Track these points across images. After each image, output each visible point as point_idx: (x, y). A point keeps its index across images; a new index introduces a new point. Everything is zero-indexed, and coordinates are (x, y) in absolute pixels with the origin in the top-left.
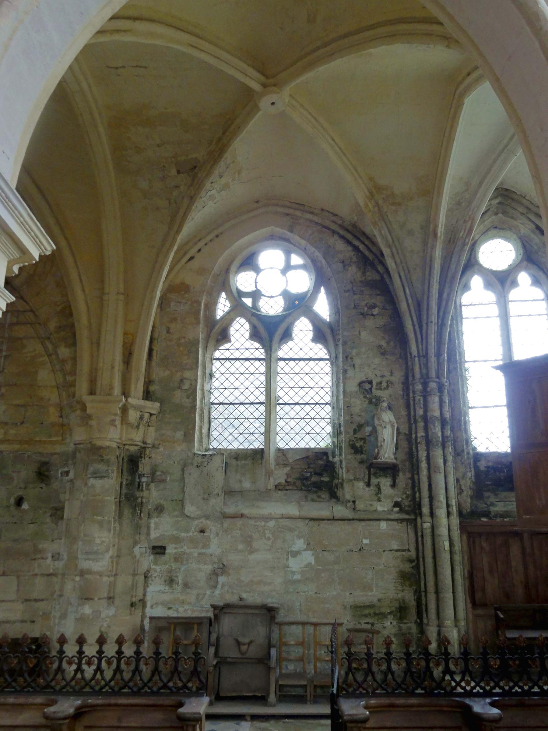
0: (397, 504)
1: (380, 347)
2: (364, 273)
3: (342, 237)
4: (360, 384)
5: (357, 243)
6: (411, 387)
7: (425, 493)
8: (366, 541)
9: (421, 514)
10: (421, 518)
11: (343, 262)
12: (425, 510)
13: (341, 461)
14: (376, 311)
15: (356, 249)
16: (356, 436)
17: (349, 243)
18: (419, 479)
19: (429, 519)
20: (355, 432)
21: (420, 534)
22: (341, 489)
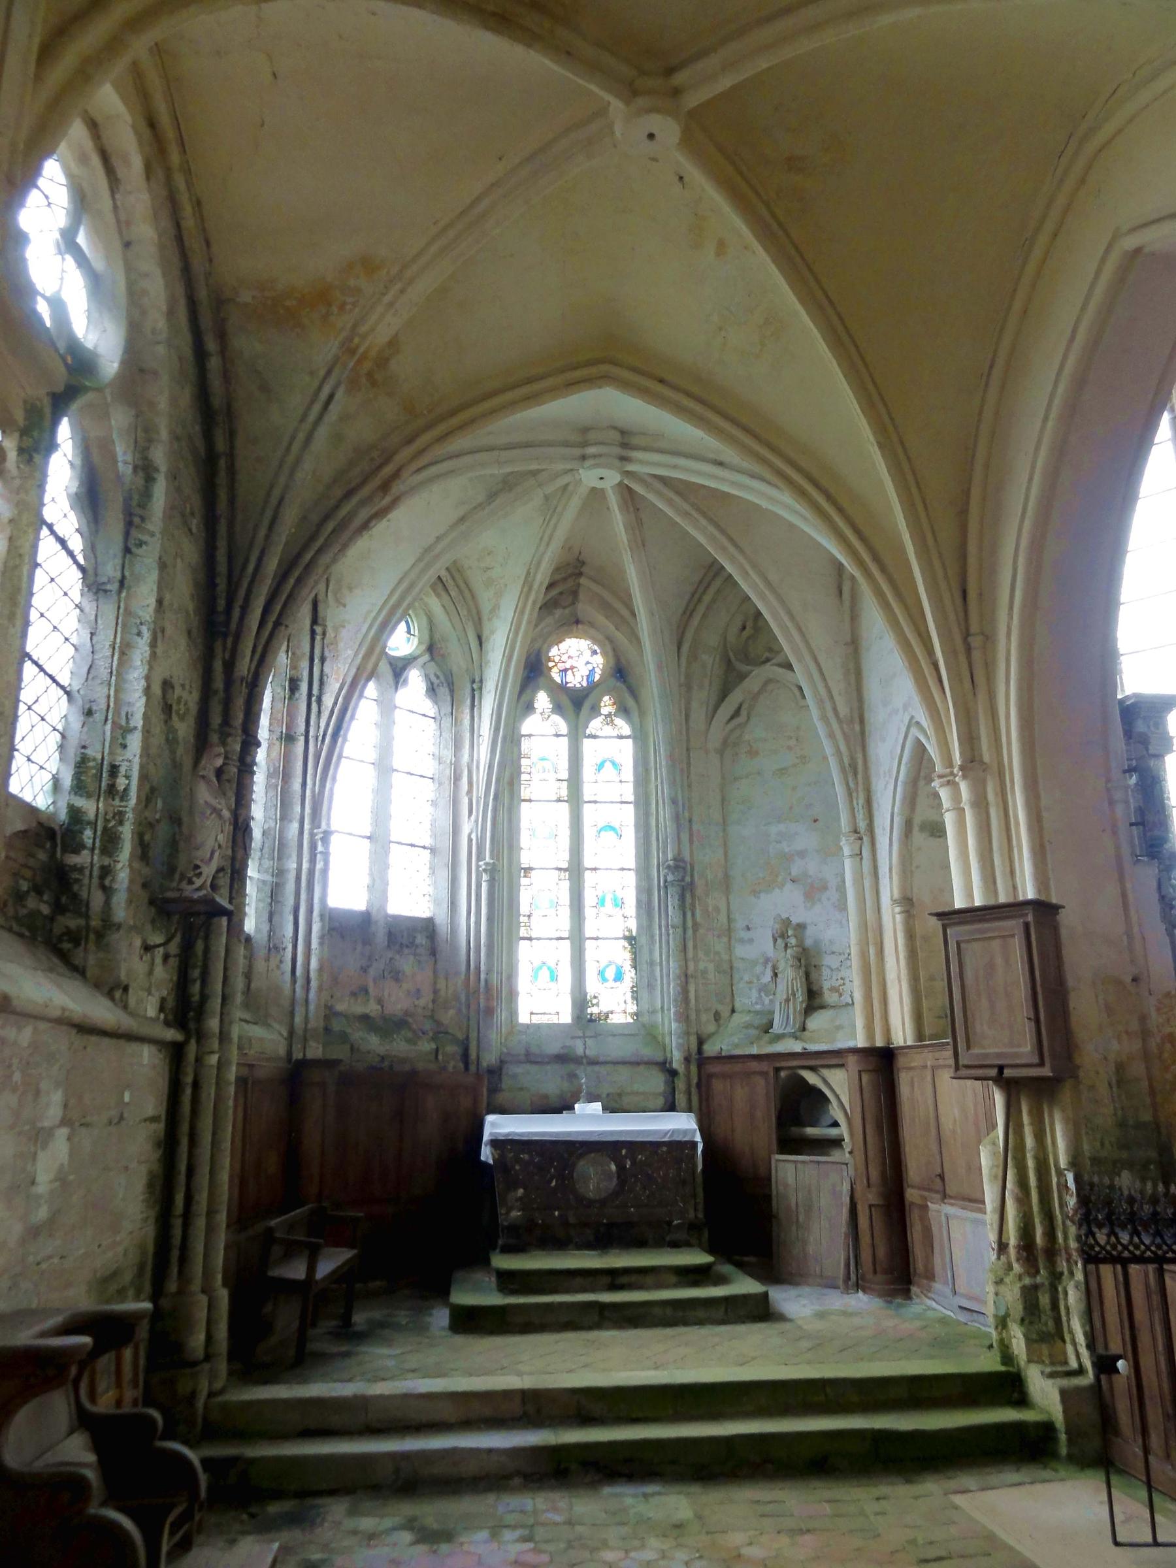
9: (201, 1036)
10: (198, 1042)
12: (213, 1024)
13: (106, 871)
16: (147, 814)
18: (207, 950)
19: (216, 1046)
22: (92, 946)
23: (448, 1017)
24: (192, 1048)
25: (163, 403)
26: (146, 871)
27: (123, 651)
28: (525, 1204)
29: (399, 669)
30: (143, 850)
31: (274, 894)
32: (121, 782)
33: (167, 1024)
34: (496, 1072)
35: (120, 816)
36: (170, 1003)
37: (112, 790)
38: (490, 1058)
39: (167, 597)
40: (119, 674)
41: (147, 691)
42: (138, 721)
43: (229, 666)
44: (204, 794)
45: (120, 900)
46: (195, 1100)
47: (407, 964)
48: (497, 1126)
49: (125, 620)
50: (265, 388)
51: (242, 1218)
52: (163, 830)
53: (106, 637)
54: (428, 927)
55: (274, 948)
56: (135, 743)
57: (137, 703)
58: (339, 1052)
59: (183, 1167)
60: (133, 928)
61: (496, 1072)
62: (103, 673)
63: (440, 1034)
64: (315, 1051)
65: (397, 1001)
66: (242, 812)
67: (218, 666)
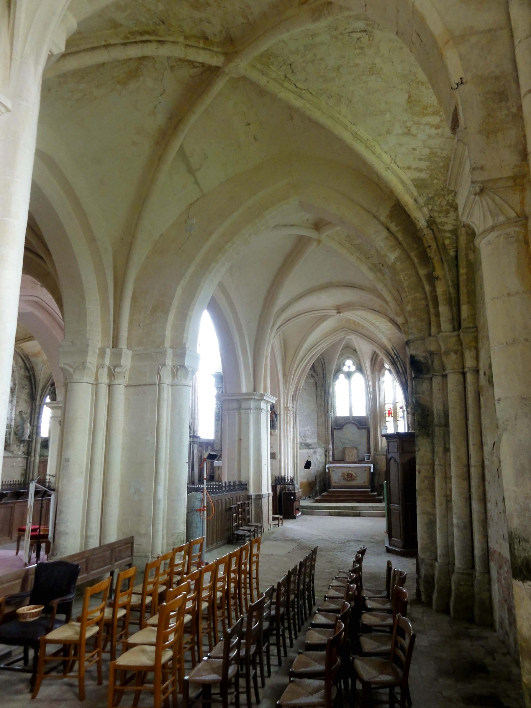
0: (23, 452)
1: (26, 400)
2: (25, 373)
3: (22, 358)
4: (20, 412)
5: (26, 362)
6: (33, 415)
7: (33, 449)
8: (14, 464)
9: (31, 456)
11: (20, 367)
12: (33, 454)
13: (10, 438)
14: (26, 387)
15: (25, 363)
17: (23, 360)
19: (33, 457)
20: (16, 428)
21: (29, 461)
24: (29, 458)
25: (17, 375)
26: (17, 437)
27: (12, 410)
30: (16, 434)
32: (12, 426)
33: (24, 455)
35: (11, 431)
36: (26, 452)
37: (11, 428)
39: (19, 400)
40: (11, 413)
41: (15, 415)
42: (14, 418)
43: (35, 404)
45: (11, 441)
46: (30, 465)
49: (12, 406)
50: (36, 364)
52: (21, 431)
53: (10, 409)
56: (13, 421)
57: (13, 416)
59: (28, 473)
60: (15, 444)
62: (9, 413)
66: (38, 425)
67: (34, 405)
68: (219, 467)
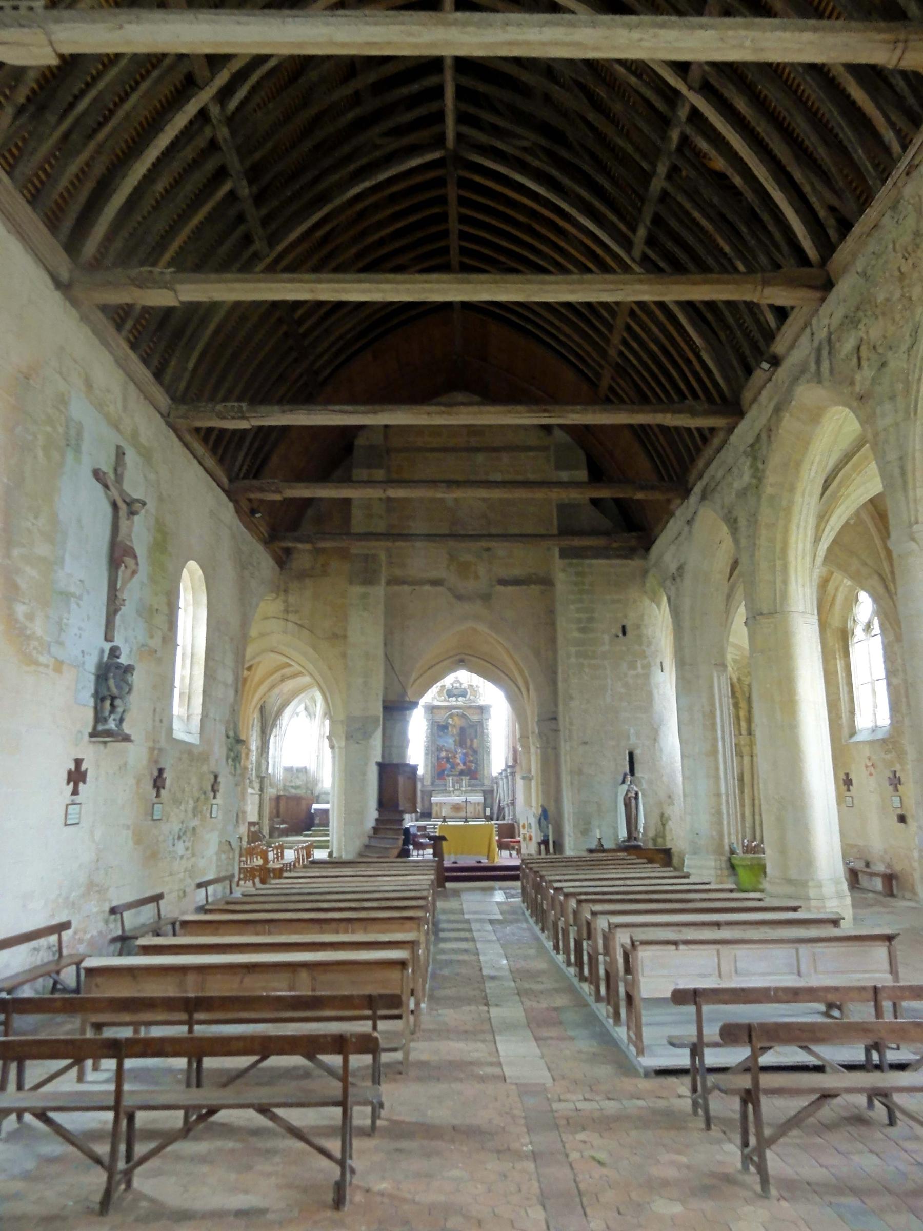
23: (309, 785)
28: (320, 820)
29: (298, 714)
31: (274, 766)
34: (318, 796)
38: (316, 793)
44: (263, 761)
47: (300, 775)
48: (315, 806)
51: (271, 819)
54: (305, 768)
55: (274, 775)
58: (287, 794)
61: (318, 796)
63: (307, 789)
64: (282, 793)
65: (299, 783)
68: (437, 804)
